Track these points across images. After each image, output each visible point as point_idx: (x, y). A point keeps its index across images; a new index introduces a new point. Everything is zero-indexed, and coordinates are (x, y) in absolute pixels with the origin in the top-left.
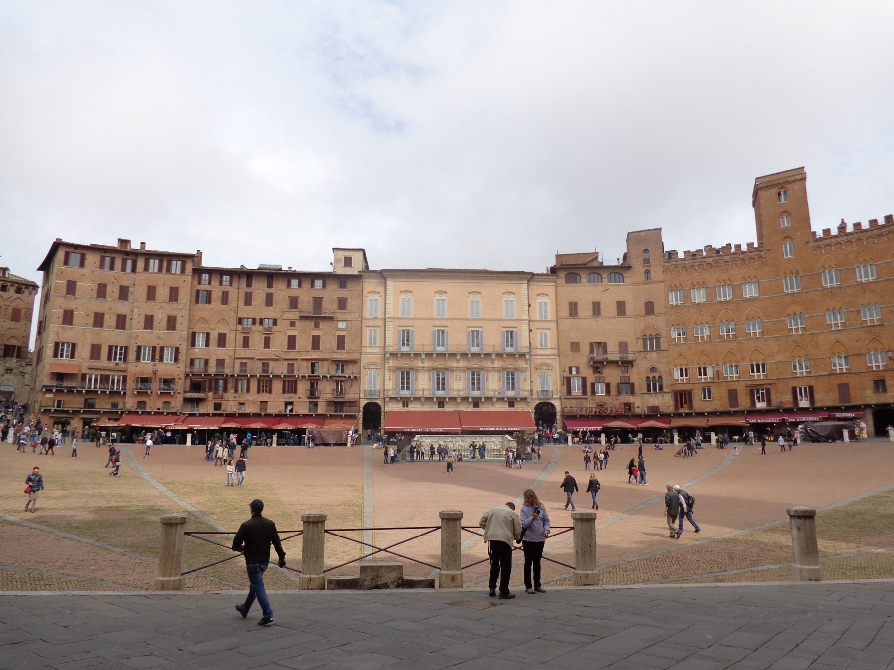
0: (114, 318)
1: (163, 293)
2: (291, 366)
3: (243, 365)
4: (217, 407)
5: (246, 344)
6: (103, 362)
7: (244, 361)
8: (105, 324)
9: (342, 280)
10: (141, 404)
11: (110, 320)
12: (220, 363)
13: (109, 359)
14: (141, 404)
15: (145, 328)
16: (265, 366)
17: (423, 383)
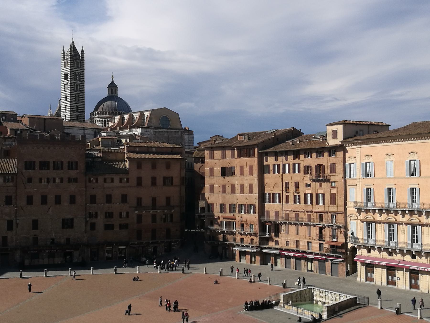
0: (230, 186)
1: (246, 170)
2: (309, 216)
3: (287, 214)
4: (277, 243)
5: (288, 202)
6: (228, 215)
7: (287, 212)
8: (227, 191)
9: (332, 150)
10: (242, 240)
11: (229, 189)
12: (277, 213)
13: (230, 211)
14: (242, 240)
15: (240, 193)
16: (297, 215)
17: (381, 234)
